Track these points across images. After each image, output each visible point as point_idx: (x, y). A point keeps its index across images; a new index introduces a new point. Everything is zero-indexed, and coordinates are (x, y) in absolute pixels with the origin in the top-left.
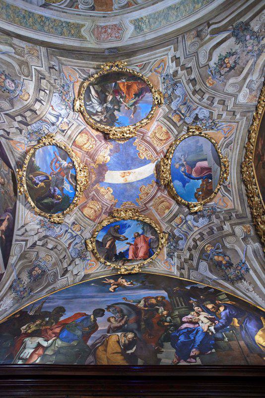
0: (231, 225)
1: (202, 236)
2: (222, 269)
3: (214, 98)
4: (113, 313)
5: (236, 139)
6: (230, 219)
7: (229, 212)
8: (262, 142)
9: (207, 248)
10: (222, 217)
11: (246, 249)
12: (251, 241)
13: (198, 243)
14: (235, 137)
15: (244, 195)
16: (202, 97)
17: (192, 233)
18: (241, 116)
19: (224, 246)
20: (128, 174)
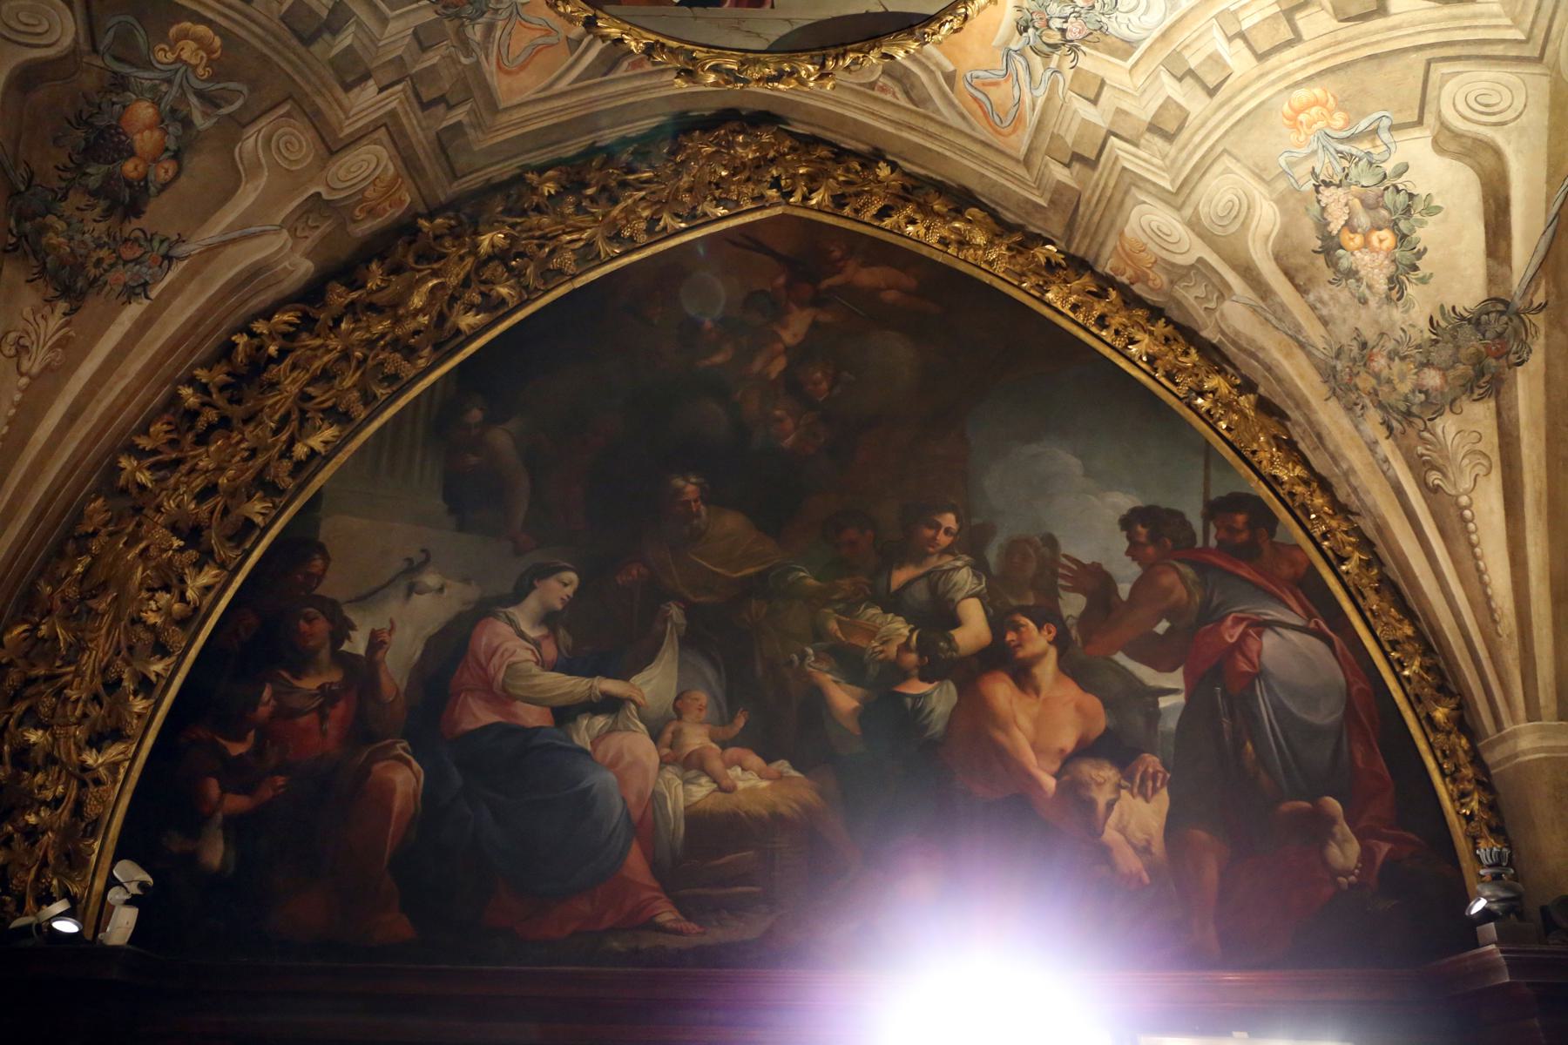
3: (1211, 92)
5: (933, 128)
6: (425, 106)
7: (474, 87)
8: (890, 296)
10: (433, 58)
11: (264, 233)
14: (943, 125)
15: (585, 141)
16: (1242, 35)
18: (1061, 188)
19: (239, 123)
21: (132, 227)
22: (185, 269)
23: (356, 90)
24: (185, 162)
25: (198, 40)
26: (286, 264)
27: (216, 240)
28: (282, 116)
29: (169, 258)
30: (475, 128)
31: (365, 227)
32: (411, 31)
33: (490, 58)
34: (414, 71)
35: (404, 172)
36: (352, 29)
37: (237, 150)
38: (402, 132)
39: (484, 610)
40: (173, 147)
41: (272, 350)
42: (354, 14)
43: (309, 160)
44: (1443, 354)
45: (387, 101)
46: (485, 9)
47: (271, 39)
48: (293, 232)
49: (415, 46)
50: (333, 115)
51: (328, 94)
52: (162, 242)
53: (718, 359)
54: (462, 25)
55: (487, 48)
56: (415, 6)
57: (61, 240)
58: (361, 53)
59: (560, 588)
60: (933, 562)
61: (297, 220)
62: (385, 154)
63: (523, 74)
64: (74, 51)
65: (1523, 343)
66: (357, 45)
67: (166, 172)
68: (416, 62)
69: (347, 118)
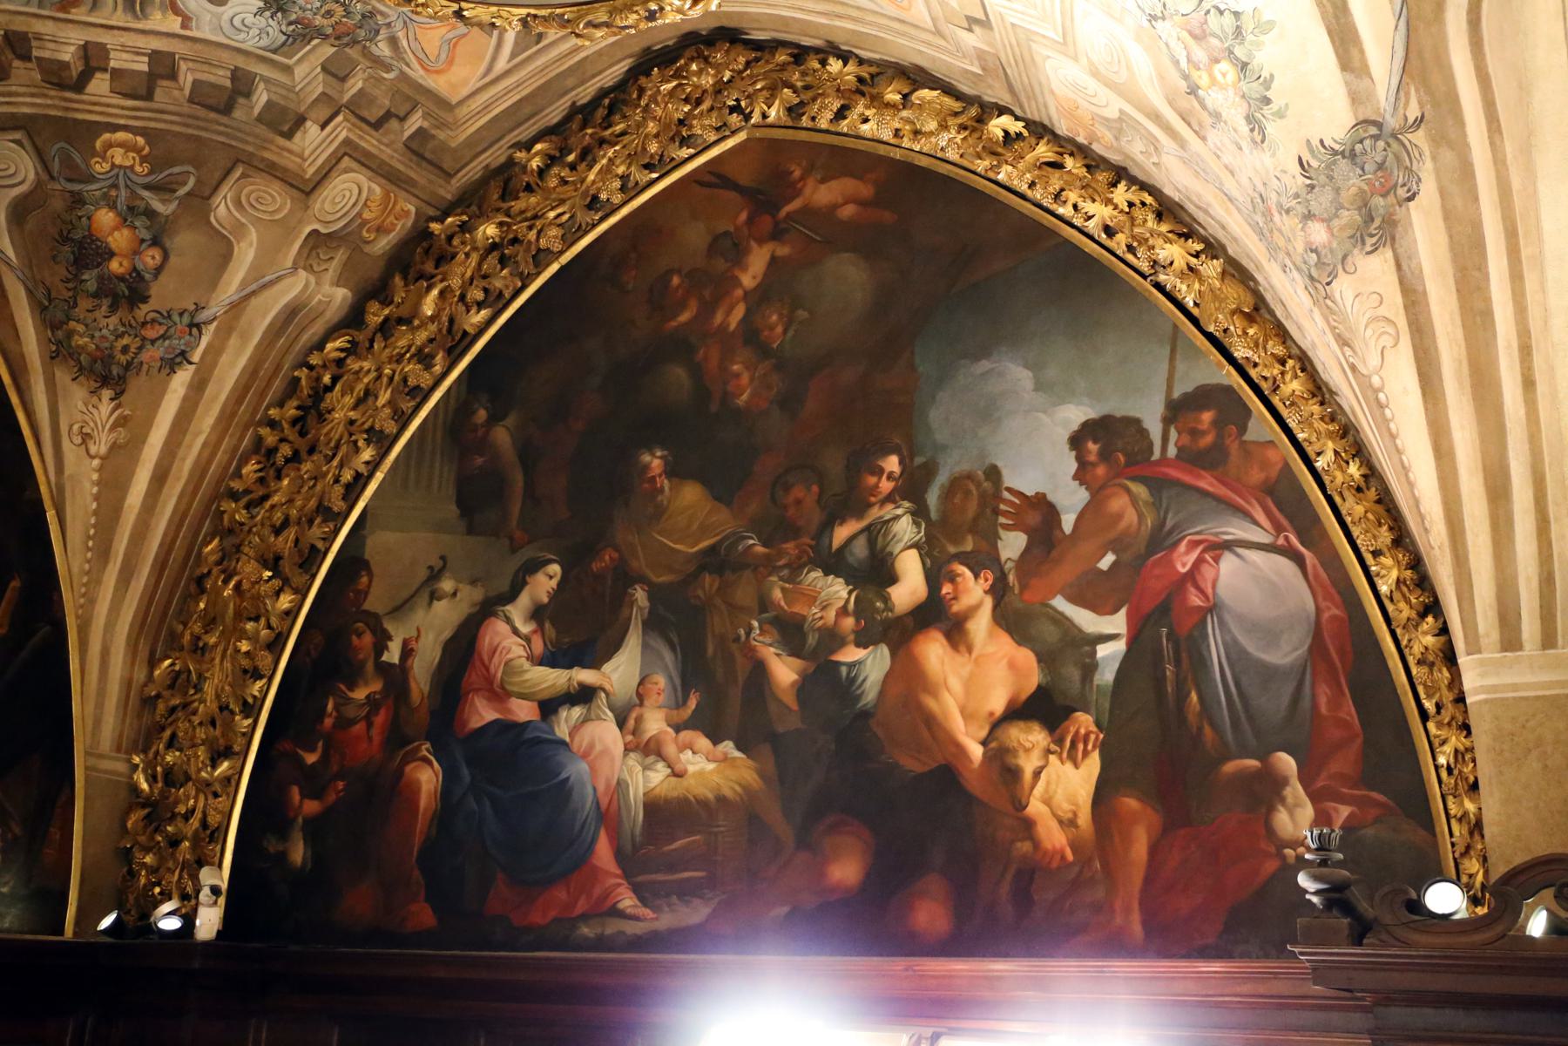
0: (348, 150)
1: (152, 78)
6: (377, 125)
7: (413, 96)
8: (848, 211)
9: (110, 145)
10: (356, 84)
11: (279, 279)
12: (334, 266)
13: (99, 85)
17: (120, 19)
19: (201, 199)
21: (143, 311)
22: (217, 328)
23: (298, 135)
24: (168, 244)
25: (121, 145)
26: (319, 296)
27: (235, 298)
28: (239, 179)
29: (196, 327)
30: (439, 128)
32: (319, 69)
33: (412, 65)
34: (345, 100)
36: (262, 86)
37: (212, 219)
38: (368, 154)
39: (487, 609)
40: (147, 236)
41: (327, 379)
42: (256, 74)
43: (288, 206)
44: (1321, 201)
45: (334, 135)
46: (376, 27)
47: (190, 121)
51: (273, 148)
52: (181, 314)
53: (684, 317)
54: (365, 47)
55: (403, 59)
56: (308, 47)
57: (86, 339)
58: (282, 102)
59: (545, 583)
60: (875, 513)
61: (308, 257)
62: (361, 178)
63: (454, 68)
64: (39, 184)
65: (1409, 170)
66: (274, 98)
67: (153, 258)
68: (342, 92)
69: (305, 160)
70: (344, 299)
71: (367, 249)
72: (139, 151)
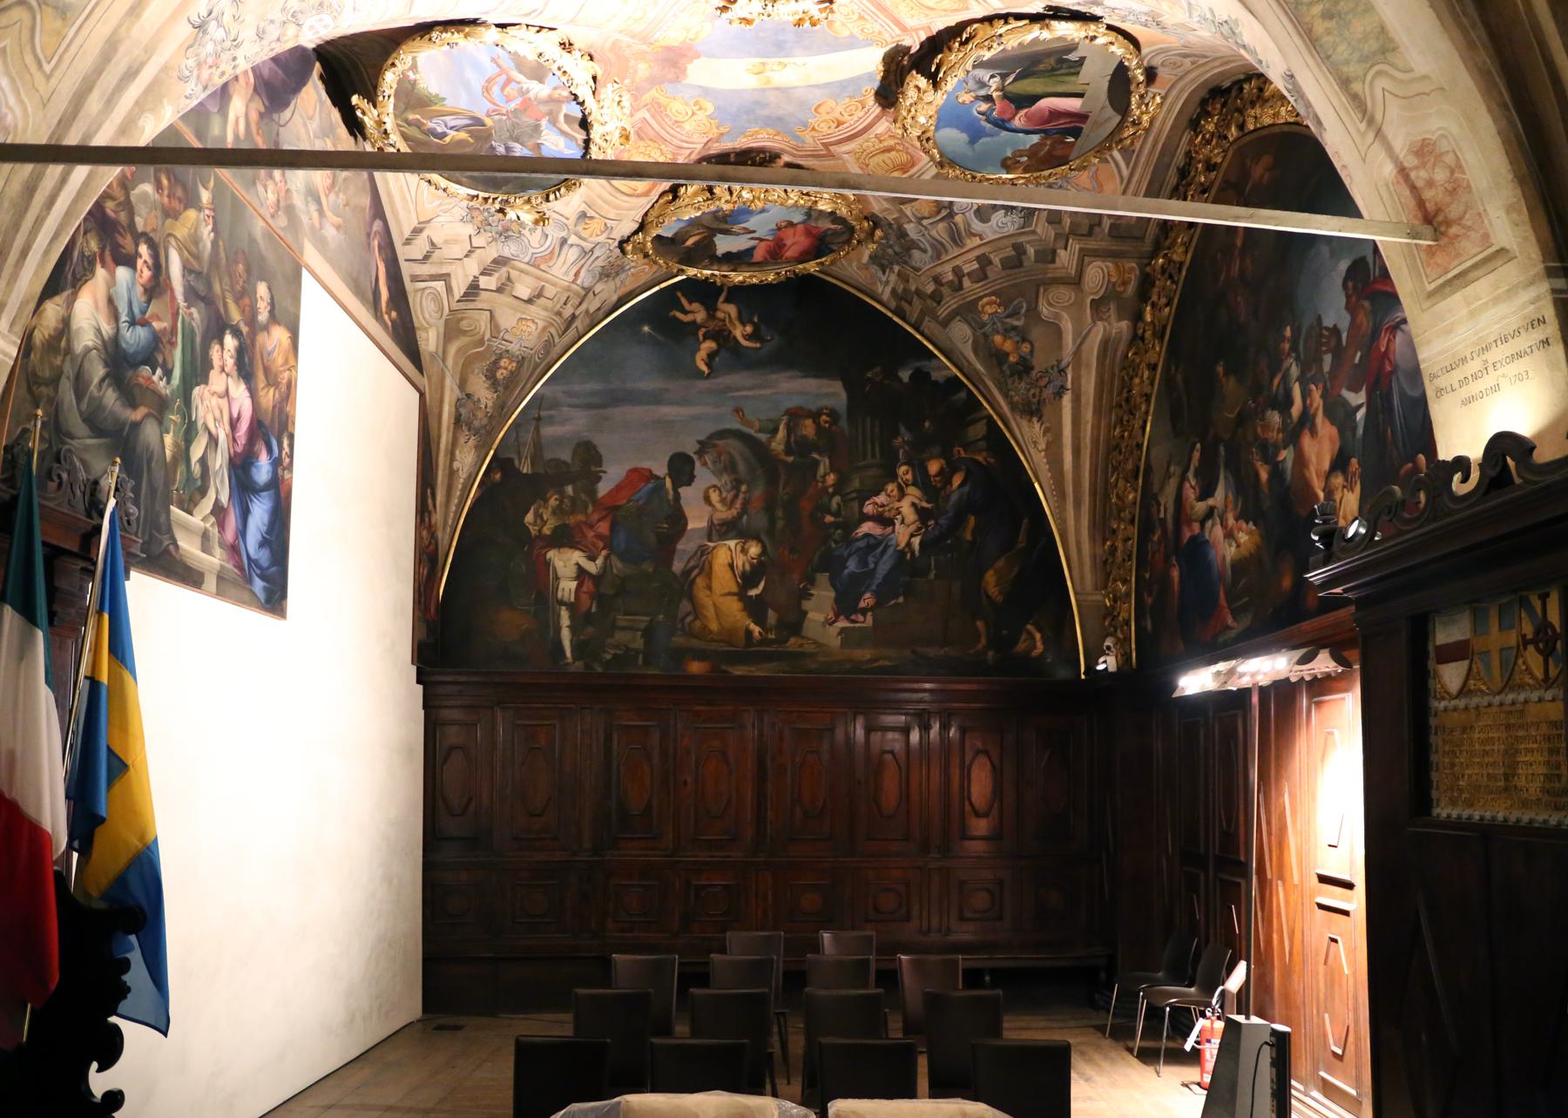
0: (1084, 253)
2: (1002, 372)
4: (713, 472)
6: (1090, 233)
9: (983, 307)
11: (1089, 331)
19: (1033, 311)
20: (775, 67)
23: (1057, 259)
25: (987, 304)
26: (1114, 331)
27: (1074, 349)
31: (1131, 289)
35: (1116, 260)
38: (1094, 251)
48: (1101, 319)
49: (1056, 226)
50: (1059, 274)
52: (1052, 368)
62: (1099, 263)
64: (974, 335)
68: (1063, 228)
70: (1128, 326)
71: (1125, 295)
72: (995, 303)
